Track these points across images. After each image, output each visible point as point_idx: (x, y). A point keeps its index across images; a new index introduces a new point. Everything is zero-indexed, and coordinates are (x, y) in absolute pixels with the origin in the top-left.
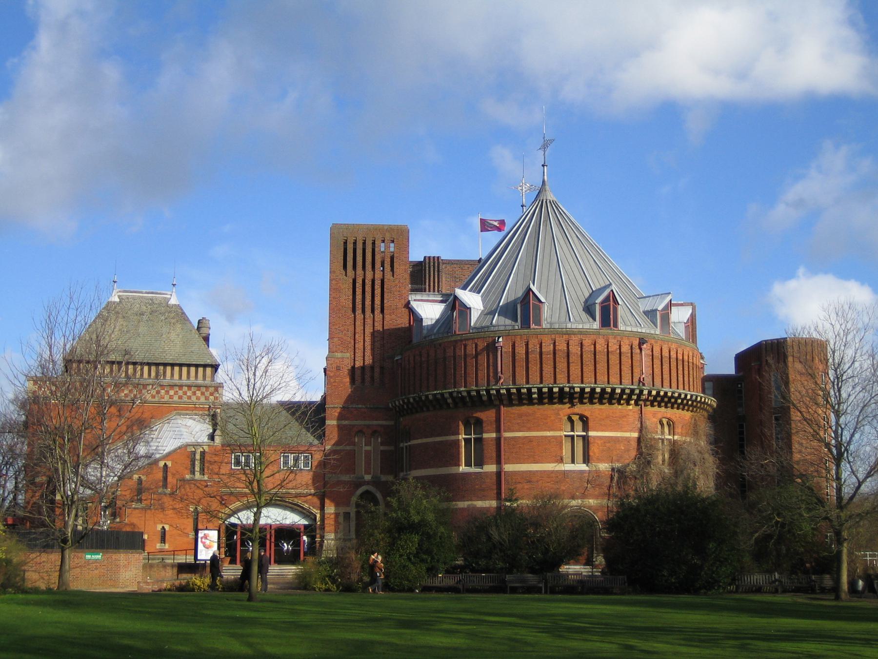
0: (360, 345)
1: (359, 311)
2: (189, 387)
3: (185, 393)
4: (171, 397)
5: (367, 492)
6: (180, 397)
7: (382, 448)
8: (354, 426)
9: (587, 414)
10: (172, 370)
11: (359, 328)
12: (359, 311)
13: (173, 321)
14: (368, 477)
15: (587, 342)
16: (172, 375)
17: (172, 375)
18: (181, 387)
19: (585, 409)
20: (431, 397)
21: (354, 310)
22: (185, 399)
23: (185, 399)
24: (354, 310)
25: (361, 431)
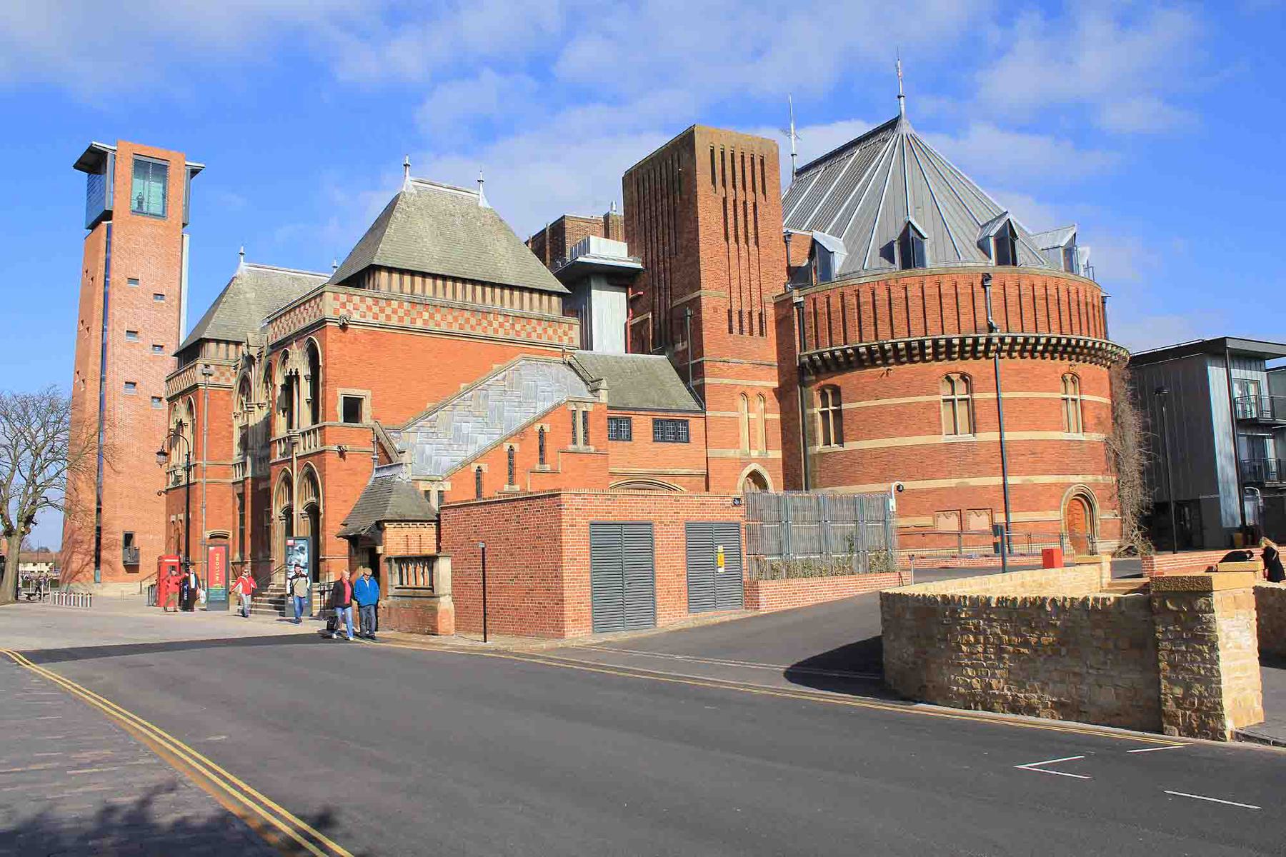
0: (735, 283)
1: (732, 240)
4: (518, 334)
9: (1079, 373)
10: (512, 294)
11: (734, 262)
12: (732, 240)
14: (754, 454)
19: (1081, 368)
21: (727, 239)
22: (534, 336)
24: (727, 239)
25: (743, 394)
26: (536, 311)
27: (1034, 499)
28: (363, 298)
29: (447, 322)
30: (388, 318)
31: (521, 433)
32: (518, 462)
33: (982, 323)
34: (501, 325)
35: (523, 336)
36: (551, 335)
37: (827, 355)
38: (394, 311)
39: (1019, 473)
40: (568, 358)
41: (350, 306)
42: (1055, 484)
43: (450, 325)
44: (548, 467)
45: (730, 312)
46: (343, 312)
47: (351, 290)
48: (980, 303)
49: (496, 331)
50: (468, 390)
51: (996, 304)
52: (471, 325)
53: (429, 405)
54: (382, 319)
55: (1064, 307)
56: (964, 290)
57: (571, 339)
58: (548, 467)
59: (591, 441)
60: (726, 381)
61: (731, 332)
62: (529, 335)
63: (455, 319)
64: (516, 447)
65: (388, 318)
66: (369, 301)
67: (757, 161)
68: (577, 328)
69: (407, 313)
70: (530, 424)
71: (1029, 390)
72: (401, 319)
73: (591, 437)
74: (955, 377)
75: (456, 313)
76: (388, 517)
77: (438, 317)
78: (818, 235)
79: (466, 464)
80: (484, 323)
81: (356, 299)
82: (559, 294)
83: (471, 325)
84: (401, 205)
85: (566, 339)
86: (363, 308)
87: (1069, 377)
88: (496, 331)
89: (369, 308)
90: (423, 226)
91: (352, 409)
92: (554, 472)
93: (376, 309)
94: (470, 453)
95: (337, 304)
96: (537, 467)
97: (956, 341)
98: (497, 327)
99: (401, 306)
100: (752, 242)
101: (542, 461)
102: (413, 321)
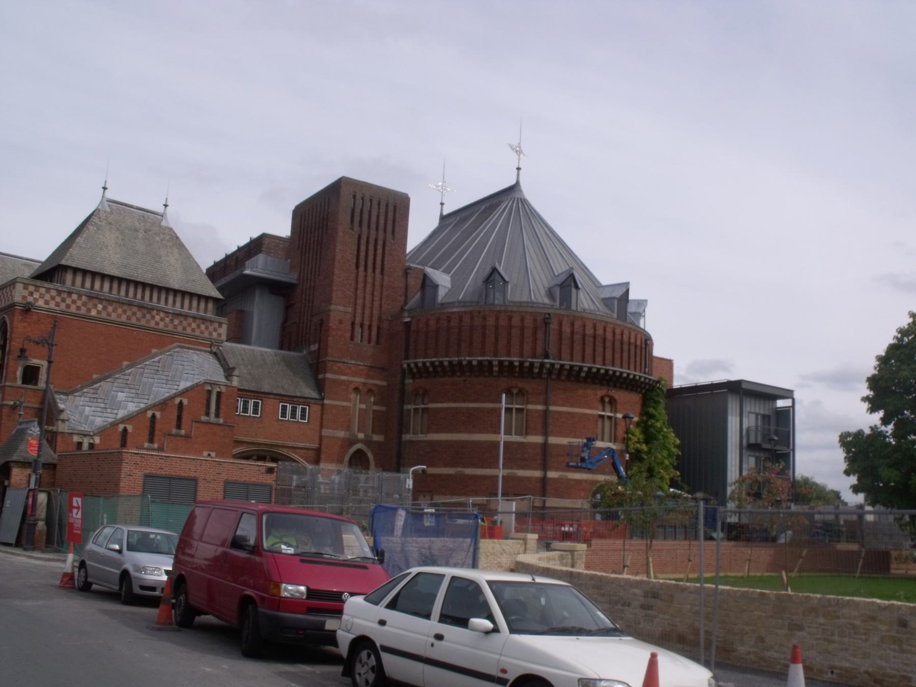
0: (360, 302)
1: (362, 268)
2: (195, 318)
3: (190, 325)
4: (175, 327)
5: (359, 451)
6: (184, 329)
7: (375, 408)
8: (351, 382)
9: (616, 397)
11: (361, 285)
12: (362, 268)
13: (169, 244)
15: (618, 331)
16: (174, 303)
17: (174, 303)
18: (186, 316)
20: (475, 363)
21: (357, 267)
22: (189, 330)
23: (189, 330)
24: (357, 267)
26: (194, 312)
27: (565, 489)
28: (48, 290)
29: (117, 314)
30: (68, 306)
31: (163, 405)
32: (158, 426)
33: (539, 350)
34: (162, 319)
35: (180, 329)
36: (202, 330)
37: (420, 365)
38: (74, 302)
39: (557, 469)
40: (214, 349)
41: (36, 295)
42: (586, 481)
43: (119, 316)
44: (183, 432)
45: (353, 324)
46: (30, 299)
47: (39, 283)
48: (540, 335)
49: (157, 324)
50: (129, 367)
51: (553, 338)
52: (137, 318)
53: (95, 376)
54: (63, 306)
55: (609, 344)
56: (528, 322)
57: (220, 335)
58: (183, 432)
59: (221, 415)
60: (344, 378)
61: (352, 338)
62: (184, 329)
63: (125, 312)
64: (158, 414)
65: (68, 306)
66: (53, 293)
67: (391, 208)
68: (225, 327)
69: (84, 304)
70: (172, 398)
71: (572, 406)
72: (78, 308)
73: (222, 412)
74: (515, 391)
75: (125, 307)
76: (14, 458)
77: (110, 309)
78: (429, 270)
79: (114, 425)
80: (148, 316)
81: (43, 290)
82: (215, 300)
83: (137, 318)
84: (95, 219)
85: (215, 334)
86: (47, 297)
87: (607, 400)
88: (157, 324)
89: (53, 298)
90: (110, 238)
91: (31, 375)
92: (187, 437)
93: (58, 299)
94: (120, 416)
95: (26, 293)
96: (174, 431)
97: (517, 364)
98: (158, 321)
99: (80, 297)
100: (378, 271)
101: (179, 426)
102: (89, 310)
